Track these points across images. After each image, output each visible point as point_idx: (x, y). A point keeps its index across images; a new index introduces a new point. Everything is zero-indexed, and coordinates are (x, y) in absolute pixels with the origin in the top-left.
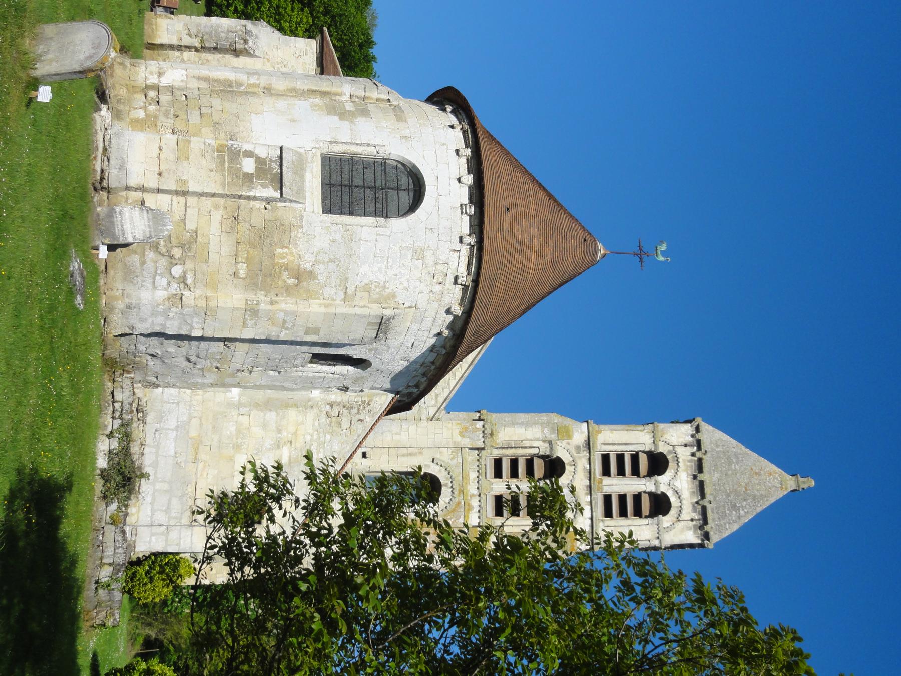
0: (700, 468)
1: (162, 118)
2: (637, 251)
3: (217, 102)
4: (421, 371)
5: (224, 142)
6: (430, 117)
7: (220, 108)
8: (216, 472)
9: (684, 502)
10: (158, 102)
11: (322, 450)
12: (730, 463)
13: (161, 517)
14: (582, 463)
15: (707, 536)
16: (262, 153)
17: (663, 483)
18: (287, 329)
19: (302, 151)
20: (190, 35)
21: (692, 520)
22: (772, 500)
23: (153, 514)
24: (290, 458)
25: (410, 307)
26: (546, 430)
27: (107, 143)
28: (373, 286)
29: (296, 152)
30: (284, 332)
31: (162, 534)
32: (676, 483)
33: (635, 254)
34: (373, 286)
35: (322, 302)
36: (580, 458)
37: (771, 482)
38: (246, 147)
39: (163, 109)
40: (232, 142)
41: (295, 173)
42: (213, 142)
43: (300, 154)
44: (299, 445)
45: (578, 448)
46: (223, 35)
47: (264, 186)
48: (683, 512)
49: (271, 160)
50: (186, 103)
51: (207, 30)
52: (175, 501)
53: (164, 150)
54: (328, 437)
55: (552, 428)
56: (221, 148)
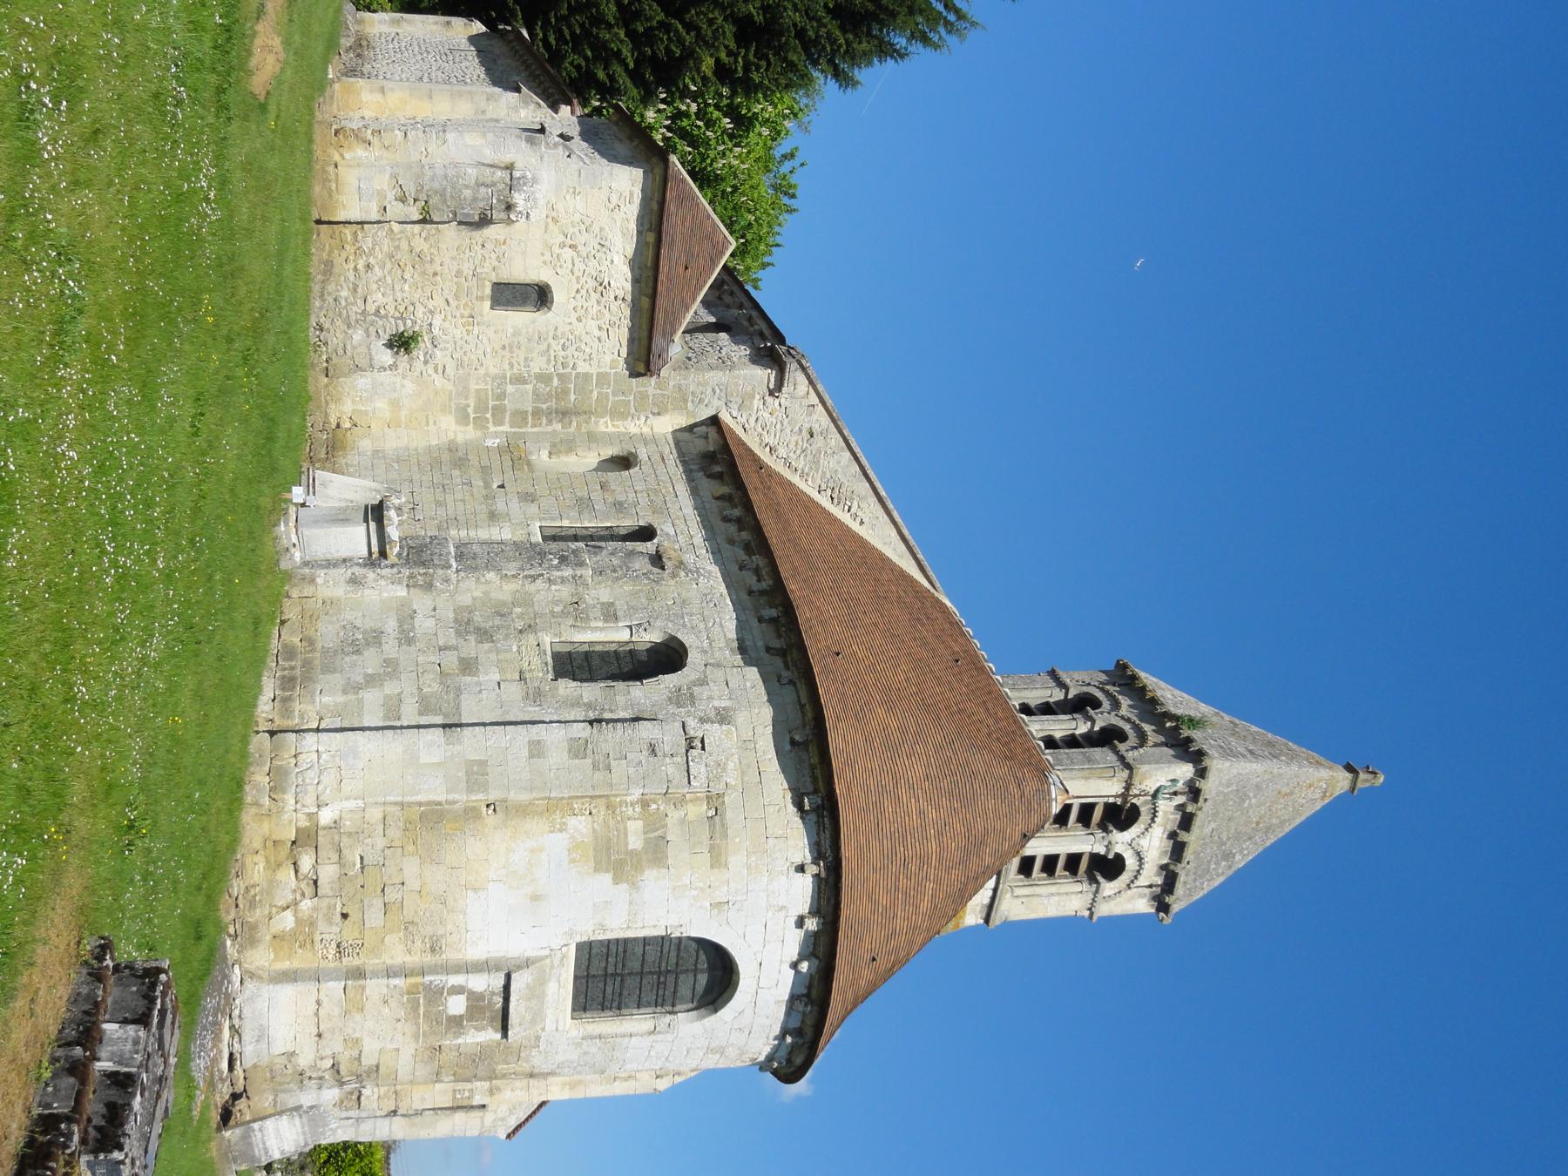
0: (1186, 822)
3: (411, 868)
6: (771, 841)
9: (1146, 866)
12: (1243, 797)
15: (1163, 907)
16: (478, 983)
20: (403, 200)
21: (1150, 886)
22: (1298, 821)
27: (236, 1022)
32: (1145, 845)
35: (567, 1079)
37: (1313, 783)
39: (324, 903)
46: (467, 193)
47: (478, 1029)
49: (493, 993)
50: (360, 881)
51: (436, 185)
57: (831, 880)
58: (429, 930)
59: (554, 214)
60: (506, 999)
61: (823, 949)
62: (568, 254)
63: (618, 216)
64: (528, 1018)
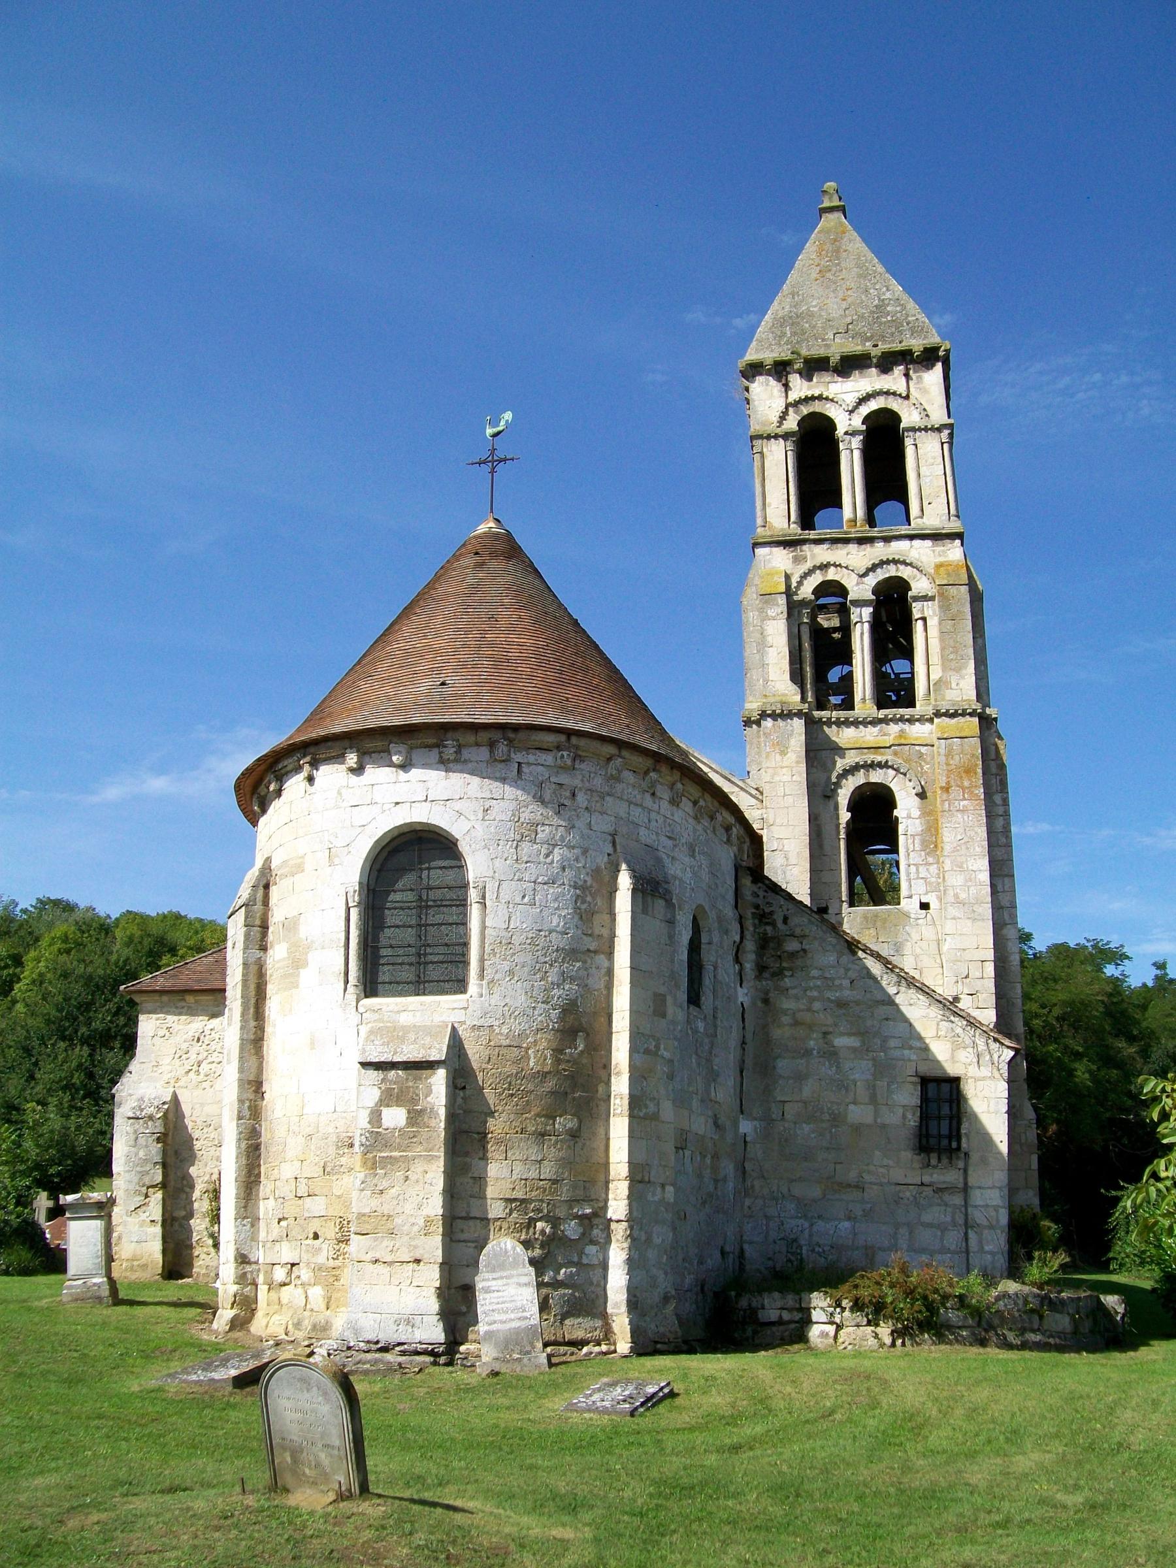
1: (321, 1259)
2: (486, 468)
4: (706, 822)
5: (358, 1157)
7: (297, 1164)
8: (877, 1153)
9: (878, 387)
10: (293, 1265)
11: (837, 982)
13: (953, 1239)
14: (822, 553)
17: (847, 423)
18: (657, 1047)
19: (364, 1030)
23: (949, 1251)
24: (850, 1034)
25: (614, 843)
26: (771, 613)
27: (374, 1347)
28: (584, 907)
29: (367, 1039)
30: (662, 1052)
31: (980, 1234)
33: (493, 472)
34: (584, 907)
36: (813, 556)
38: (363, 1121)
39: (305, 1257)
40: (357, 1144)
41: (402, 1039)
42: (361, 1176)
43: (371, 1032)
44: (830, 1021)
45: (797, 560)
46: (141, 1154)
47: (429, 1092)
48: (894, 388)
52: (927, 1217)
53: (378, 1256)
54: (815, 973)
55: (766, 602)
56: (369, 1164)
57: (312, 749)
58: (332, 1150)
59: (172, 1081)
60: (393, 1065)
61: (372, 744)
62: (205, 1067)
63: (176, 1027)
64: (428, 1040)
